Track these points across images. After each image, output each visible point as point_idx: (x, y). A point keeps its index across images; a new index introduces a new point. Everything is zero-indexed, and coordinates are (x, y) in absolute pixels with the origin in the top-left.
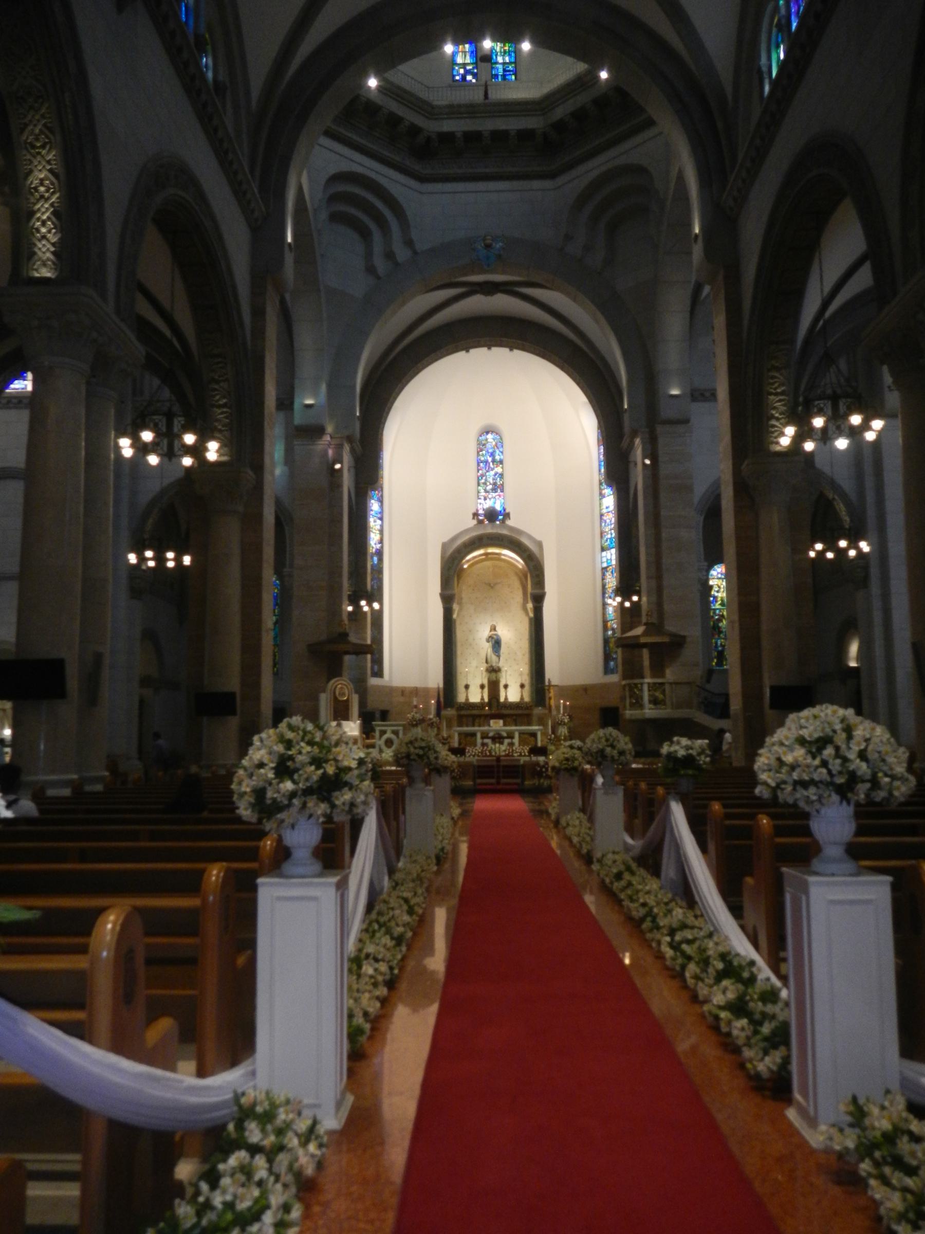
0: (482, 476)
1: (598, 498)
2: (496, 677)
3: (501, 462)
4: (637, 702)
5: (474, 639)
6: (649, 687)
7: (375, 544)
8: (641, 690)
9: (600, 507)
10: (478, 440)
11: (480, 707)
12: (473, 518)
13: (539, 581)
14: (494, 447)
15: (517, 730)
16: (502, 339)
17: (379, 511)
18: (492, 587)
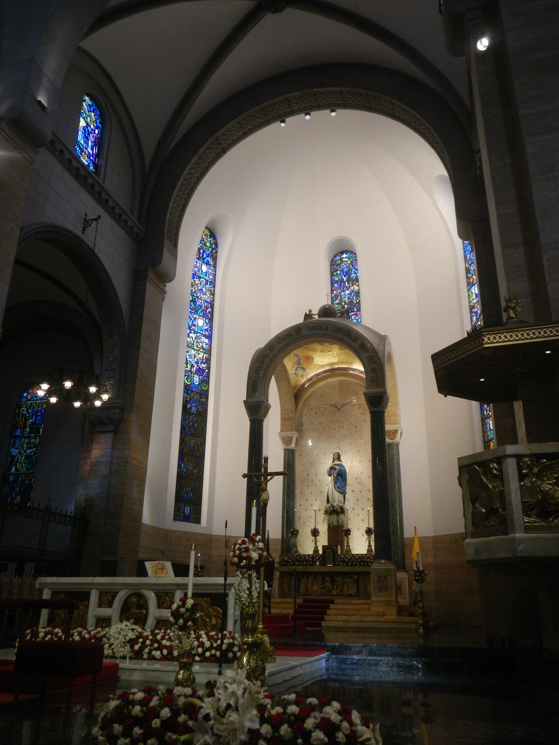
0: (336, 296)
1: (466, 290)
2: (338, 520)
3: (357, 280)
4: (492, 512)
5: (316, 474)
6: (520, 469)
7: (197, 363)
8: (501, 477)
9: (469, 299)
10: (332, 261)
11: (309, 561)
12: (305, 319)
13: (377, 376)
14: (349, 266)
16: (316, 90)
17: (207, 328)
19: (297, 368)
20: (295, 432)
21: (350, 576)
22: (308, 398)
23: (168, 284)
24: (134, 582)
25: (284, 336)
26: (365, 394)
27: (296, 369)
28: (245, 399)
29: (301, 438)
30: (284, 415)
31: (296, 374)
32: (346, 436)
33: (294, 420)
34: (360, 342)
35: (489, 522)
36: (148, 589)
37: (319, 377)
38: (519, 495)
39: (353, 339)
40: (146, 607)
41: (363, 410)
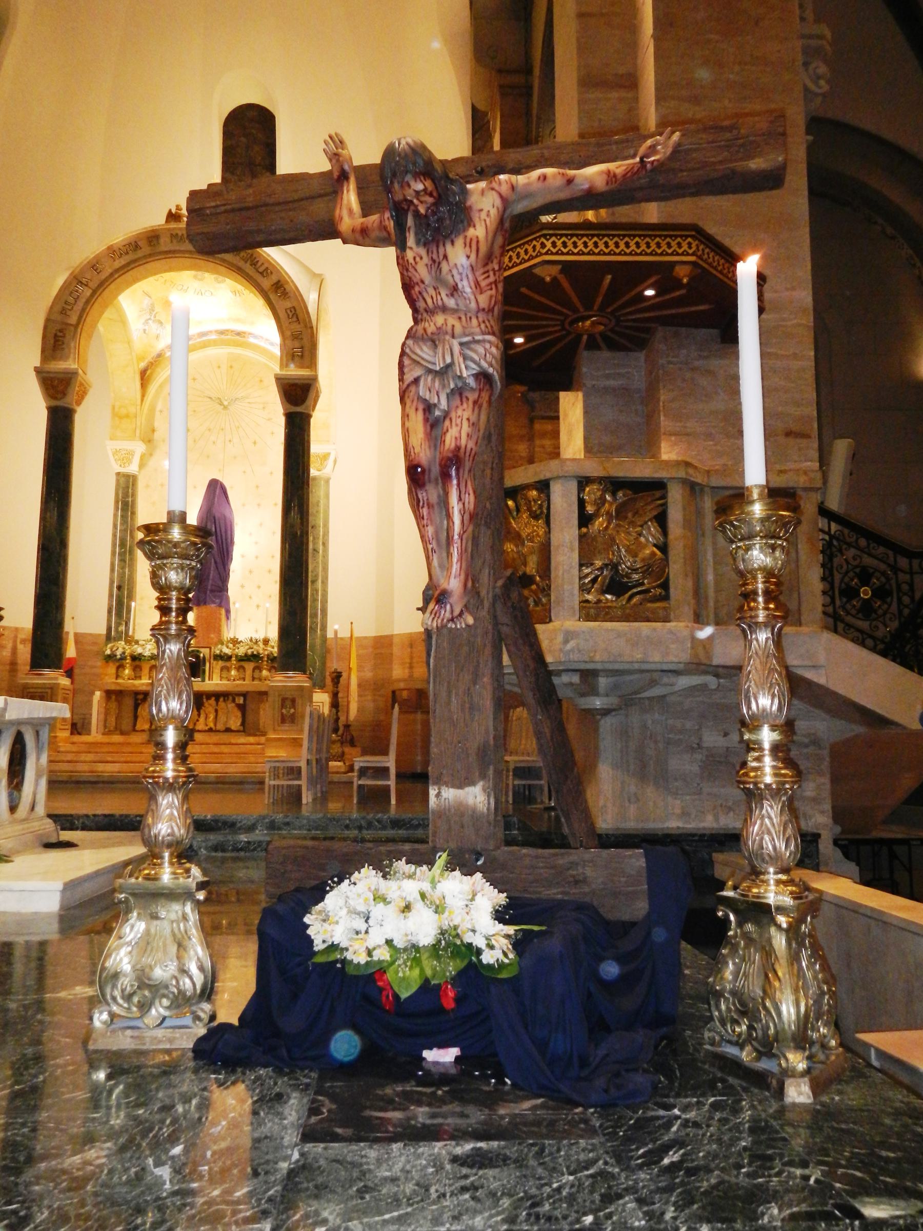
6: (581, 503)
18: (225, 408)
21: (231, 698)
26: (279, 380)
27: (146, 322)
28: (38, 365)
29: (151, 455)
32: (235, 457)
34: (274, 279)
38: (577, 552)
39: (261, 270)
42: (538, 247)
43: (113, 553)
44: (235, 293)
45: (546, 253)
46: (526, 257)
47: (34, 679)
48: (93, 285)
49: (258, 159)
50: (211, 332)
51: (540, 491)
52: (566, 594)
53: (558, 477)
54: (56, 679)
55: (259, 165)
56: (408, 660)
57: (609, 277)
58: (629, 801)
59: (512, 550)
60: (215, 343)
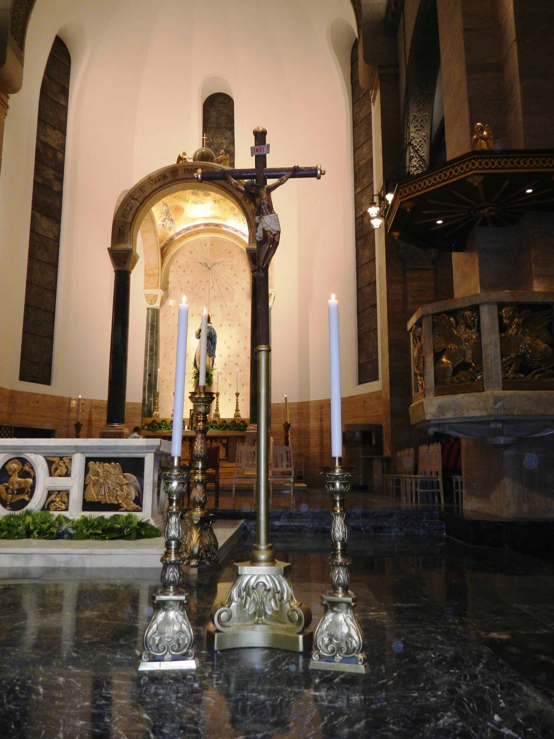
6: (500, 318)
15: (78, 449)
18: (209, 269)
19: (165, 219)
20: (161, 290)
21: (219, 440)
22: (175, 254)
23: (11, 96)
24: (16, 444)
25: (158, 176)
27: (164, 220)
28: (110, 247)
30: (149, 270)
31: (163, 226)
32: (215, 298)
33: (160, 276)
35: (458, 378)
36: (35, 453)
37: (189, 231)
38: (499, 348)
40: (32, 474)
41: (235, 271)
42: (470, 165)
43: (146, 355)
44: (215, 201)
45: (476, 169)
46: (462, 172)
47: (109, 429)
48: (141, 199)
49: (223, 125)
50: (200, 224)
51: (473, 311)
52: (494, 374)
53: (486, 303)
54: (122, 429)
55: (224, 128)
56: (319, 417)
57: (508, 182)
58: (524, 502)
59: (455, 348)
60: (203, 231)
